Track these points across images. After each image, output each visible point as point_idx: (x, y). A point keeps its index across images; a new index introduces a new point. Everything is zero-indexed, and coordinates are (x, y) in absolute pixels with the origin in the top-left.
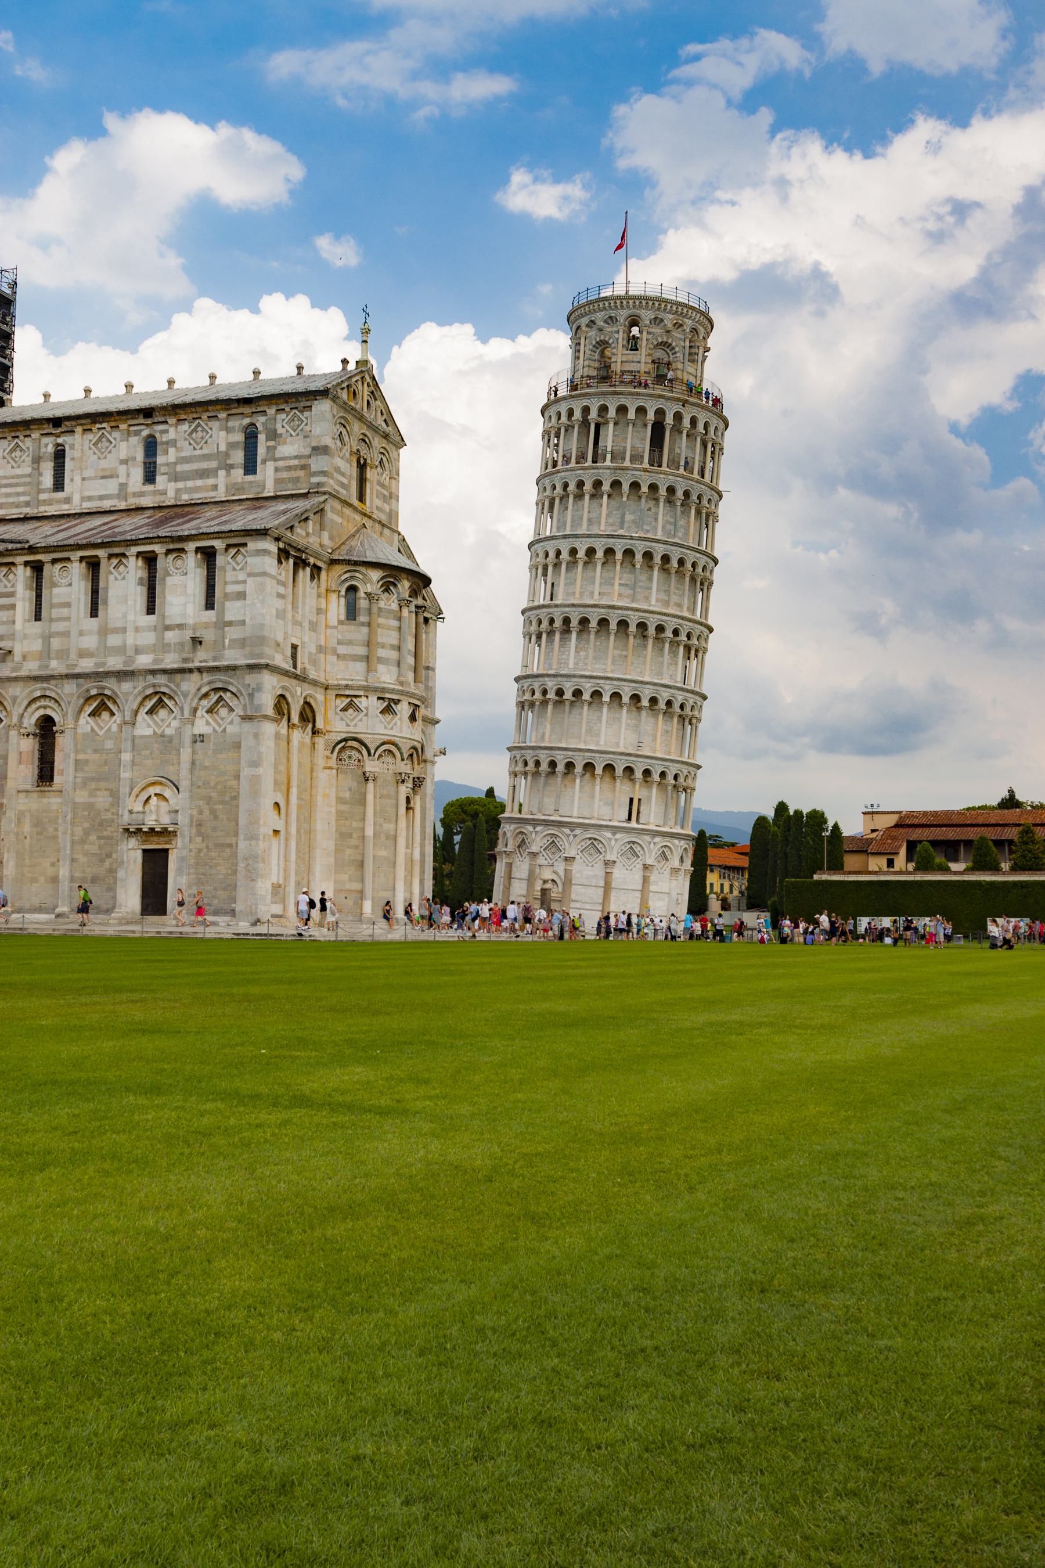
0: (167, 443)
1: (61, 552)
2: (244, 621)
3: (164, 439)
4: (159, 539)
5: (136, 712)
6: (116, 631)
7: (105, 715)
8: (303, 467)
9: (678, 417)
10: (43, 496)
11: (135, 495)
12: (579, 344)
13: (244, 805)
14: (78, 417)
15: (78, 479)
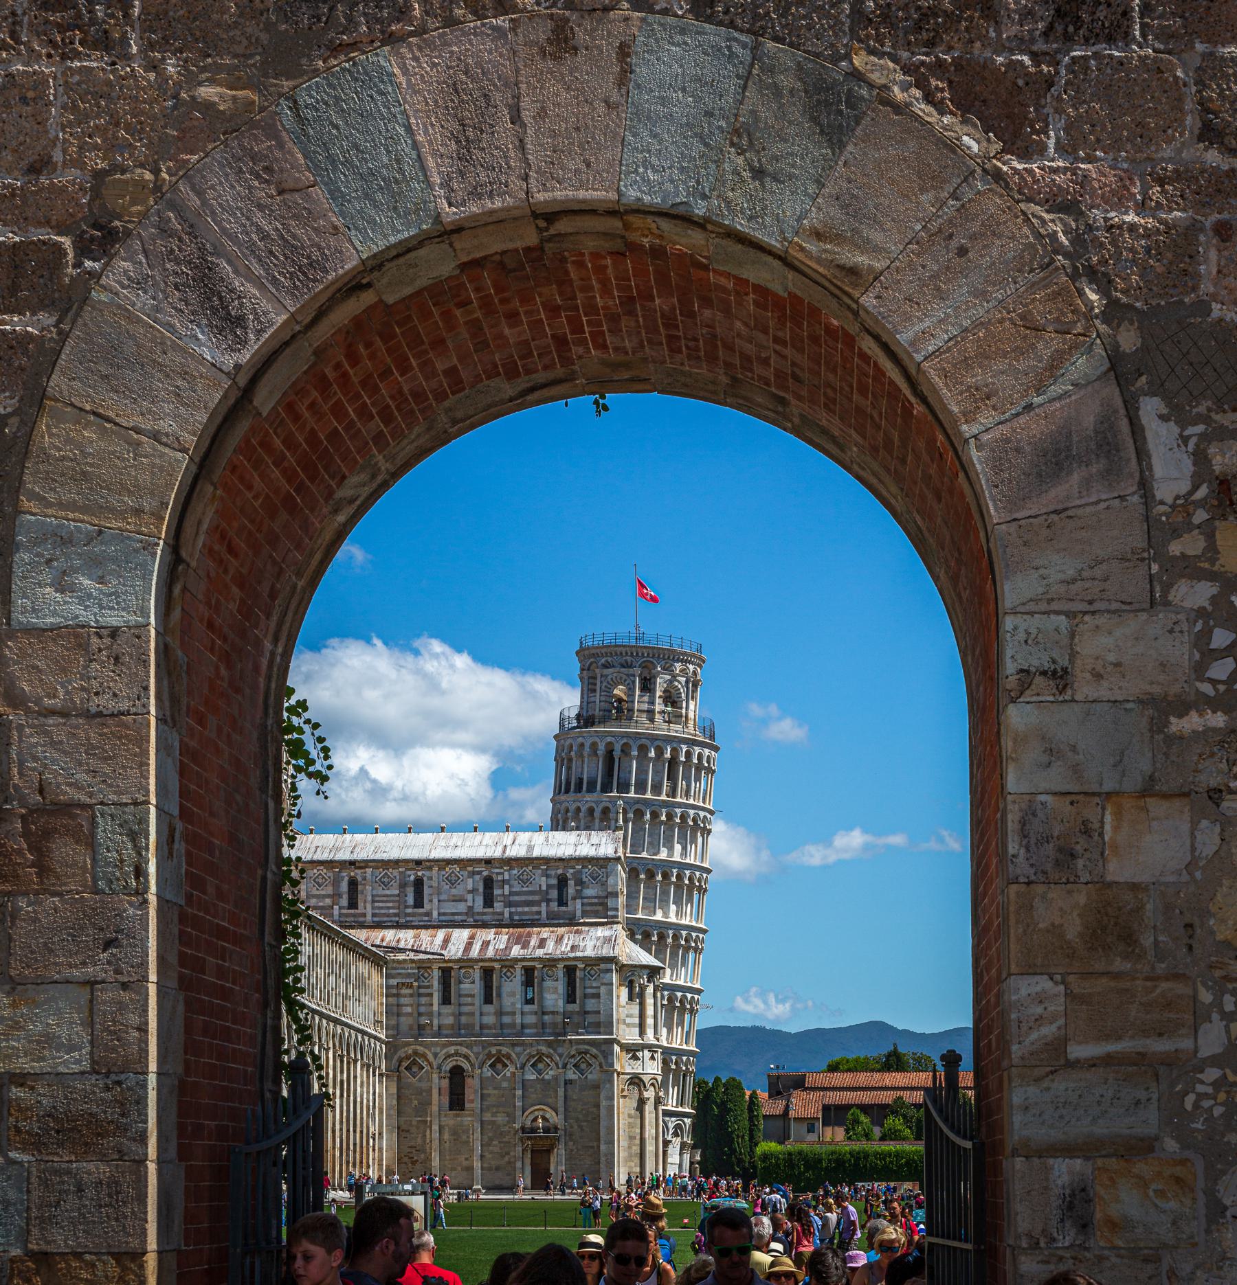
0: (503, 881)
1: (465, 963)
2: (599, 1012)
3: (500, 878)
4: (539, 959)
5: (523, 1067)
6: (508, 1013)
7: (499, 1066)
8: (601, 904)
9: (688, 754)
10: (409, 910)
11: (478, 914)
12: (595, 678)
13: (603, 1123)
14: (438, 860)
15: (435, 901)
